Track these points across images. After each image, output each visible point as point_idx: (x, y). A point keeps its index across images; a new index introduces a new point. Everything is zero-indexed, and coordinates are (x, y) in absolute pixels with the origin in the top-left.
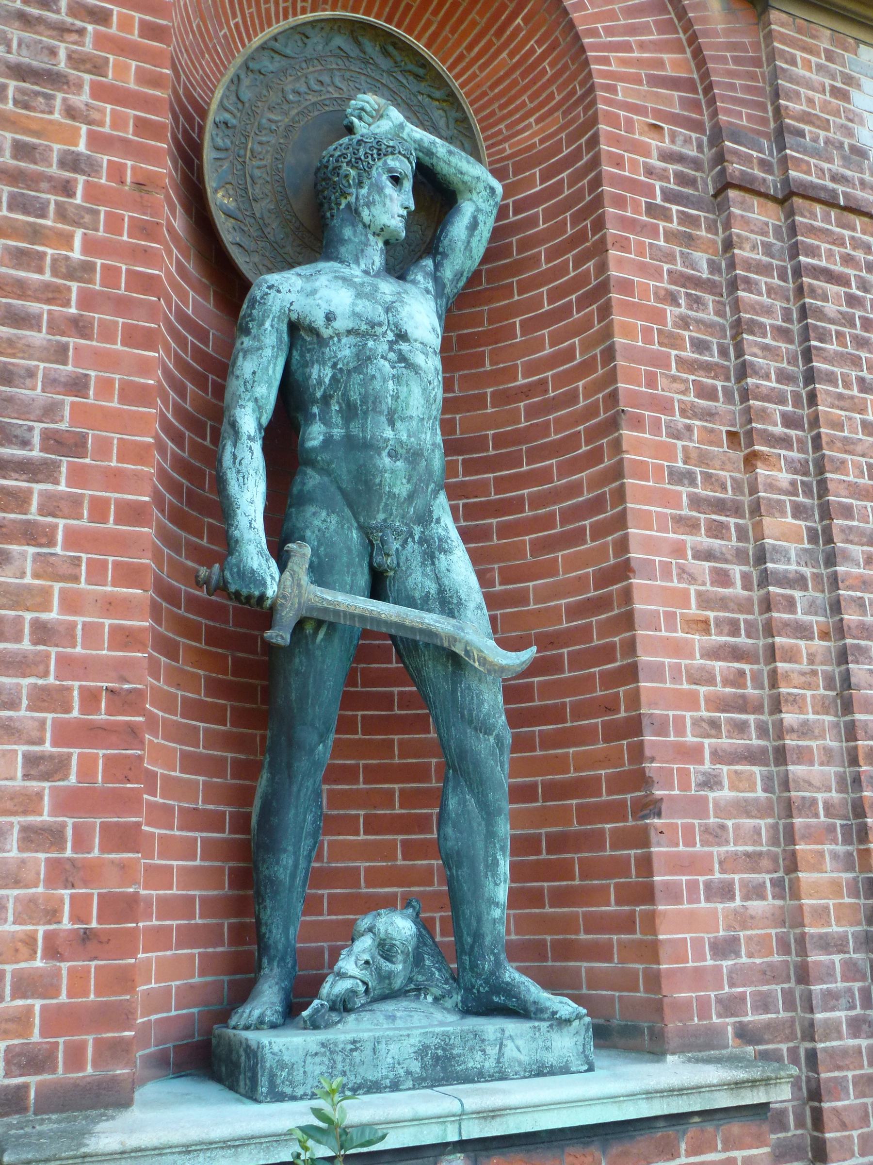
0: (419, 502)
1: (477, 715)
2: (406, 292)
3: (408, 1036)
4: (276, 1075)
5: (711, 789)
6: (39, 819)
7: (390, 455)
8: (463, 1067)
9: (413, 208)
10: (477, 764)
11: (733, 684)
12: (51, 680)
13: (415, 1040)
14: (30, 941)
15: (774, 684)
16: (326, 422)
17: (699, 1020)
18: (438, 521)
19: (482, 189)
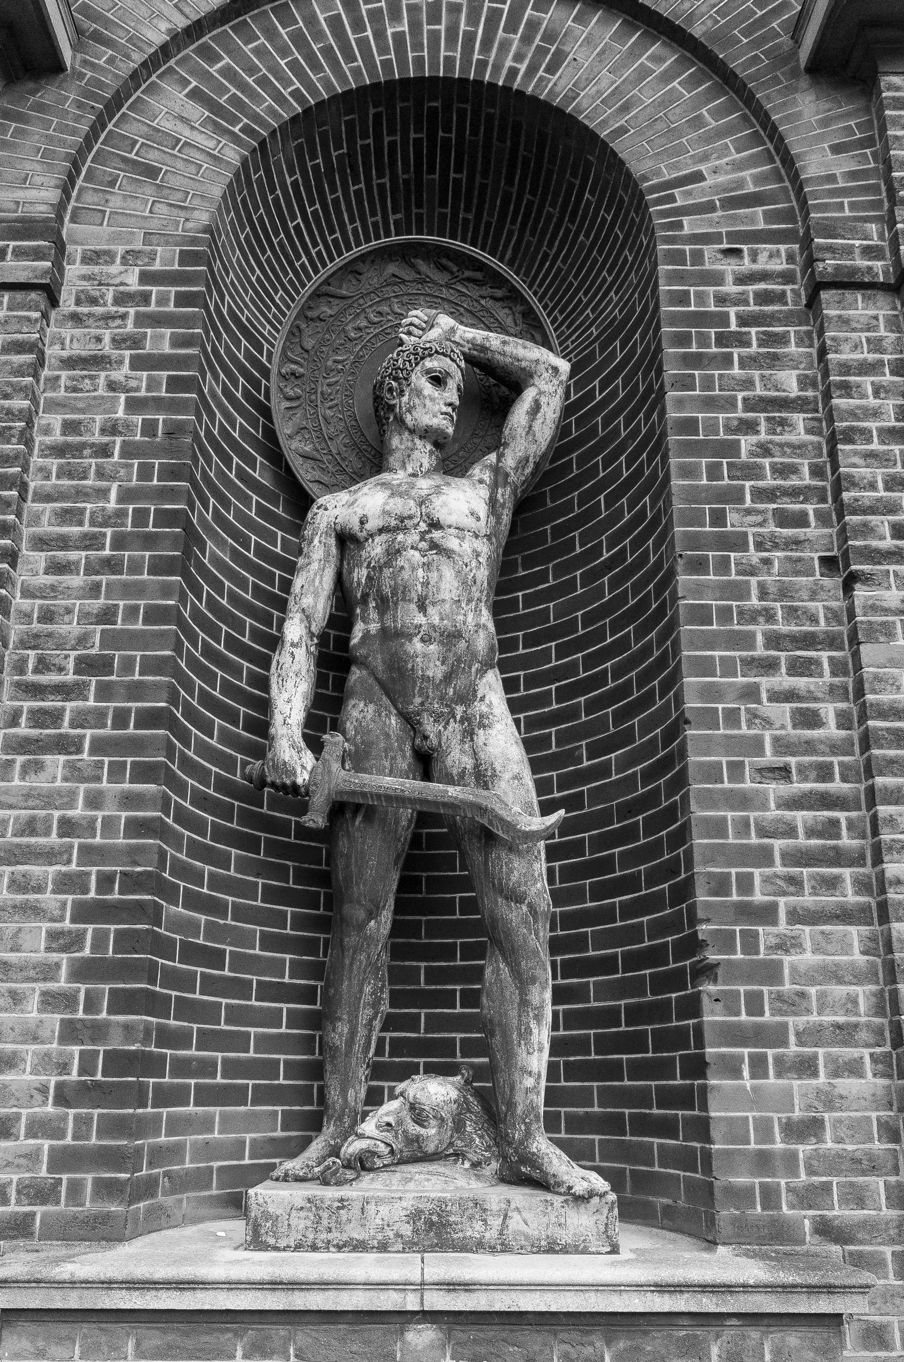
0: (460, 682)
1: (507, 884)
2: (448, 484)
3: (400, 1198)
4: (260, 1225)
5: (787, 951)
6: (57, 985)
7: (422, 640)
8: (460, 1235)
9: (458, 403)
10: (508, 934)
11: (820, 835)
12: (73, 867)
13: (409, 1203)
14: (43, 1090)
15: (875, 832)
16: (365, 621)
17: (763, 1209)
18: (482, 699)
19: (544, 371)
